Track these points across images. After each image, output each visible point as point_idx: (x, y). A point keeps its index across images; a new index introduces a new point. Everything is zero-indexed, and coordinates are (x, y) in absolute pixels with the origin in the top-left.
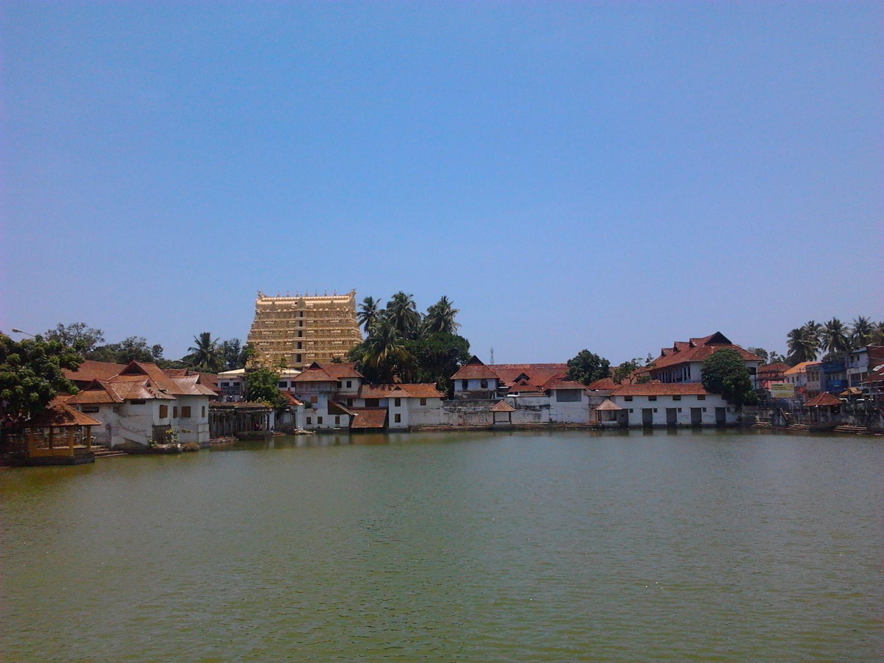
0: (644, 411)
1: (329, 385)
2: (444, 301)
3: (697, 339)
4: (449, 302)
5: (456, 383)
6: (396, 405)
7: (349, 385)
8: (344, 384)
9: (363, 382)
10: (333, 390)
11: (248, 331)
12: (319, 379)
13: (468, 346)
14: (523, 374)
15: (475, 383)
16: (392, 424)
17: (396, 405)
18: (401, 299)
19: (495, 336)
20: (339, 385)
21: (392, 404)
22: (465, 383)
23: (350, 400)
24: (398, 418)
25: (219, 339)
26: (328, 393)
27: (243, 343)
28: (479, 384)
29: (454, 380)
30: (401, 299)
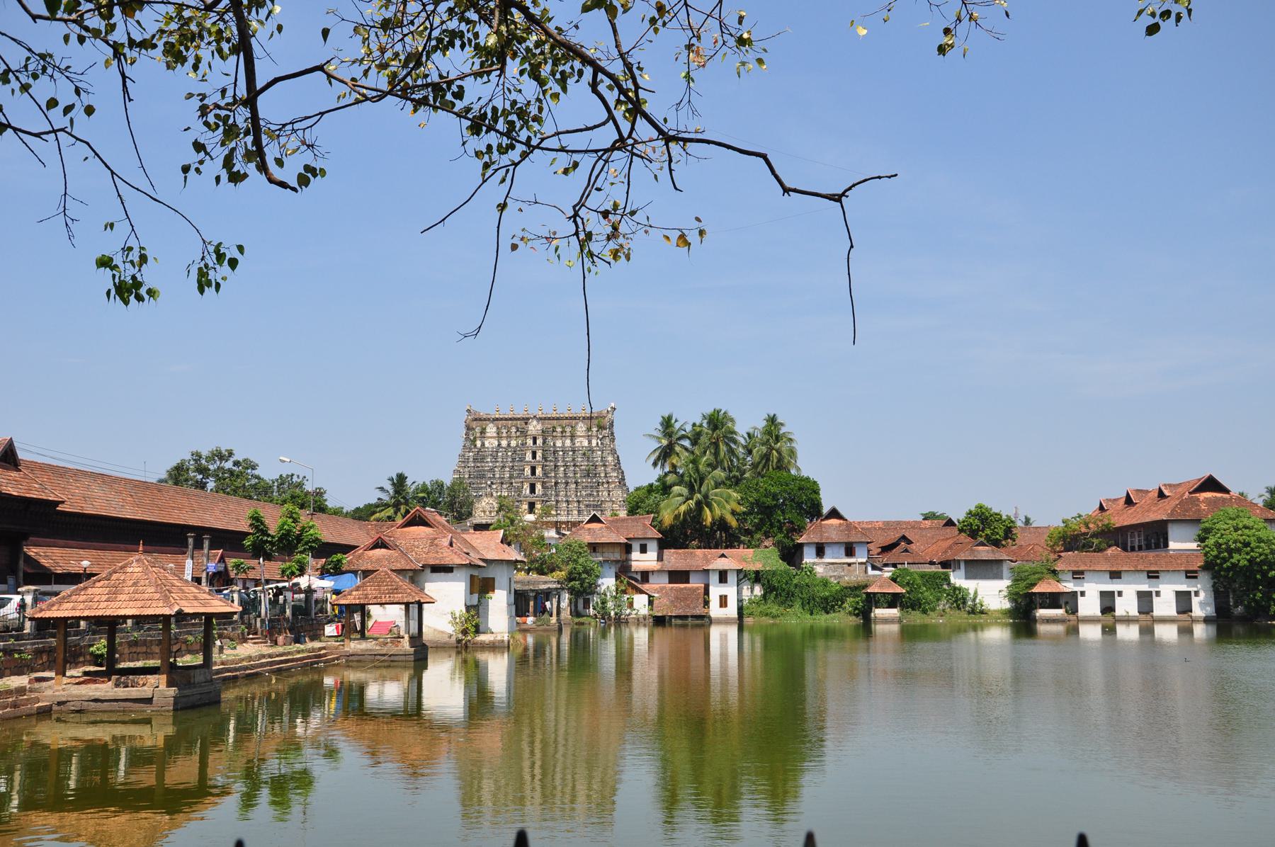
0: (1103, 594)
1: (617, 549)
2: (772, 420)
3: (1170, 485)
4: (779, 420)
5: (806, 550)
6: (721, 581)
7: (643, 550)
8: (636, 546)
9: (663, 545)
10: (617, 556)
11: (454, 462)
12: (604, 540)
13: (816, 492)
14: (904, 538)
15: (836, 548)
16: (715, 610)
17: (721, 581)
18: (716, 421)
19: (868, 479)
20: (628, 548)
21: (714, 578)
22: (820, 551)
23: (645, 576)
24: (723, 601)
25: (418, 477)
26: (617, 562)
27: (448, 482)
28: (842, 551)
29: (801, 546)
30: (716, 421)
